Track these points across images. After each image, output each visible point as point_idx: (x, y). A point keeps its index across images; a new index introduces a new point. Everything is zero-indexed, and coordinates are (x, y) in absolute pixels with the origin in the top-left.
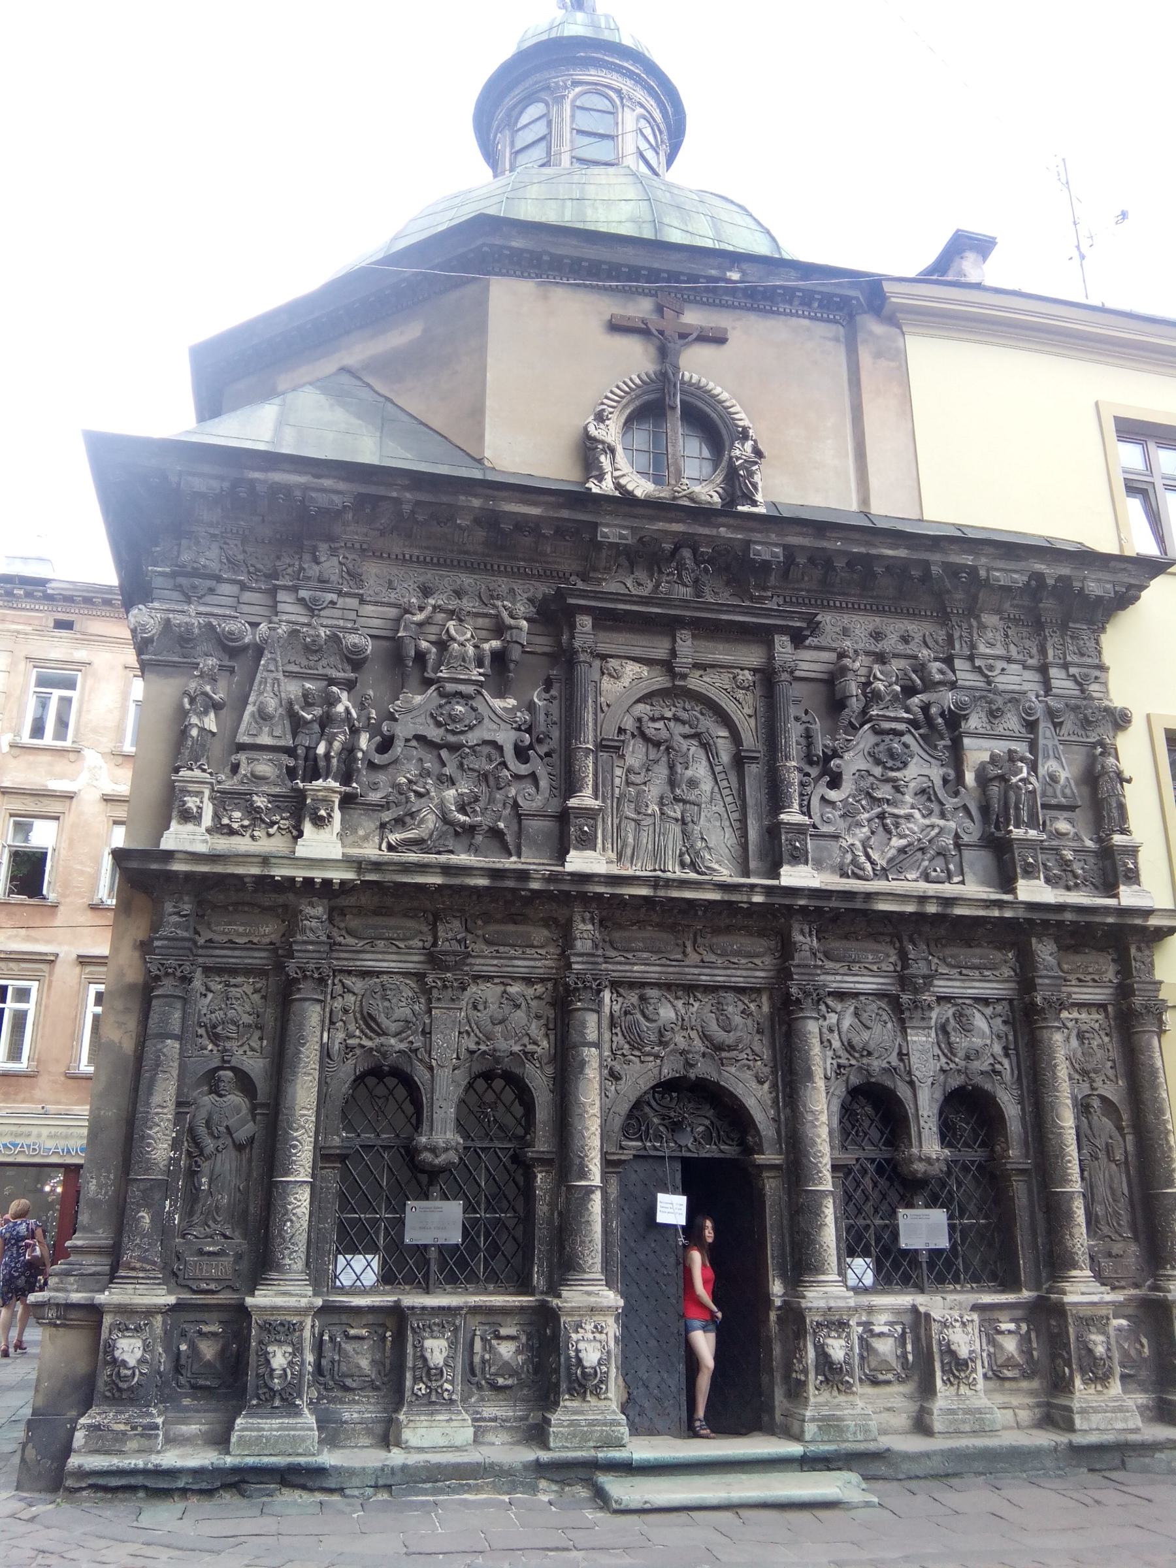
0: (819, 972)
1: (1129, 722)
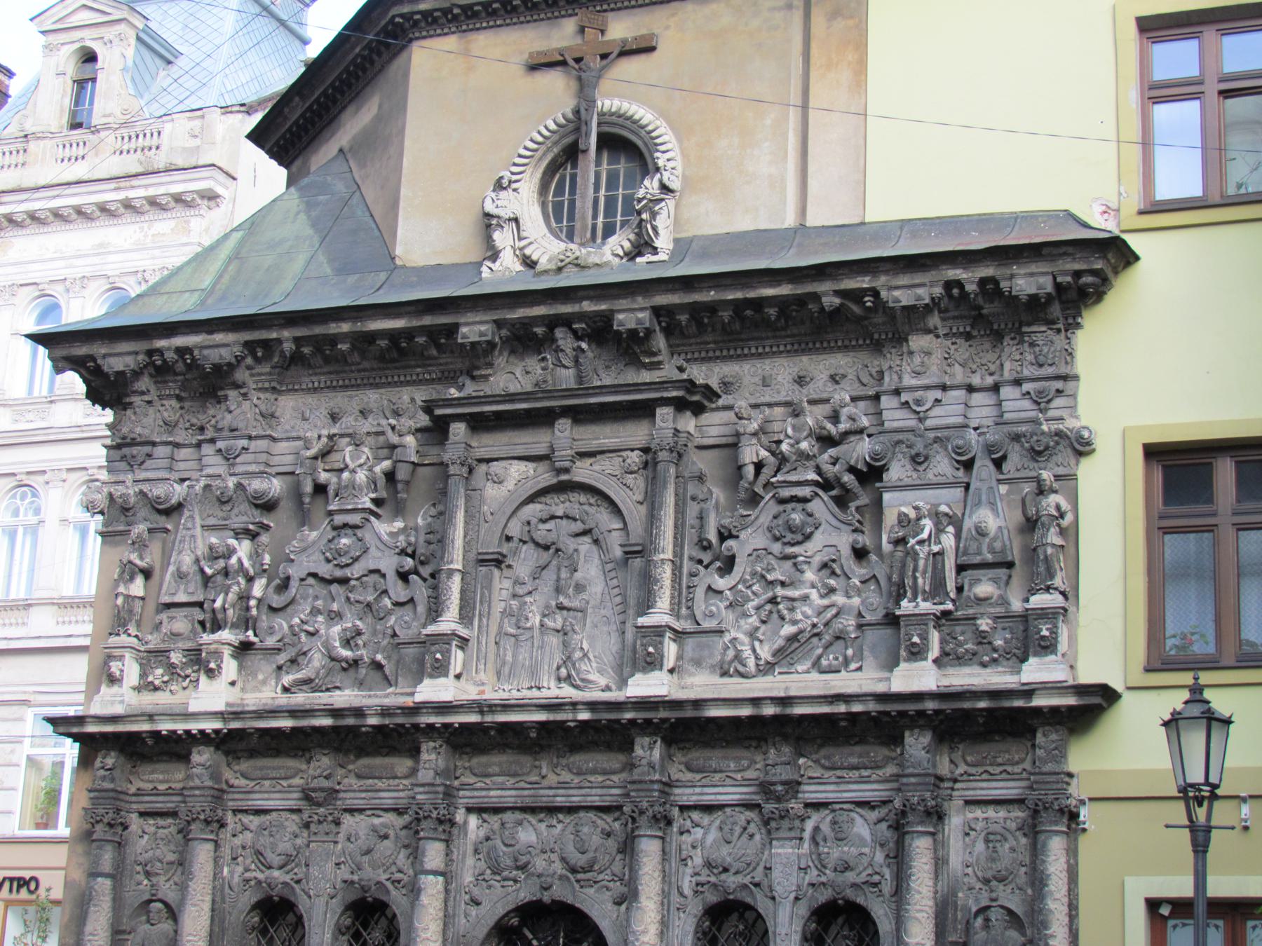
1: (1089, 444)
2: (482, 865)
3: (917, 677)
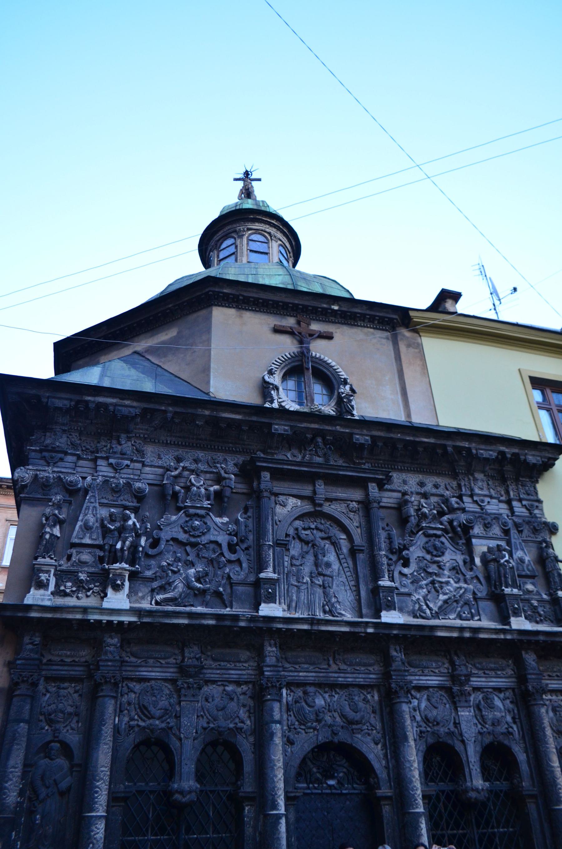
0: (407, 674)
3: (519, 623)
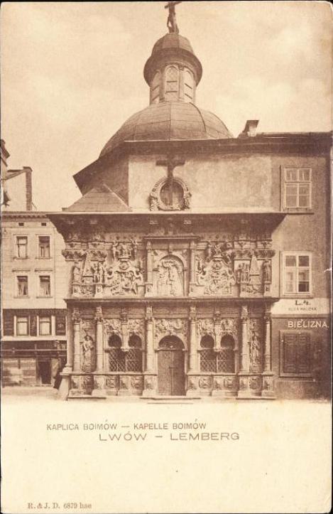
2: (158, 329)
3: (244, 295)
